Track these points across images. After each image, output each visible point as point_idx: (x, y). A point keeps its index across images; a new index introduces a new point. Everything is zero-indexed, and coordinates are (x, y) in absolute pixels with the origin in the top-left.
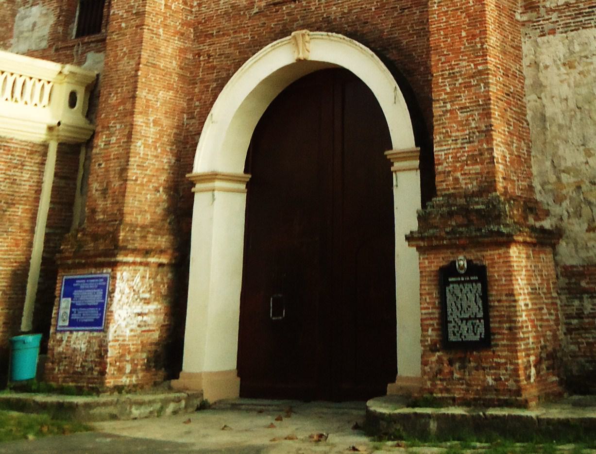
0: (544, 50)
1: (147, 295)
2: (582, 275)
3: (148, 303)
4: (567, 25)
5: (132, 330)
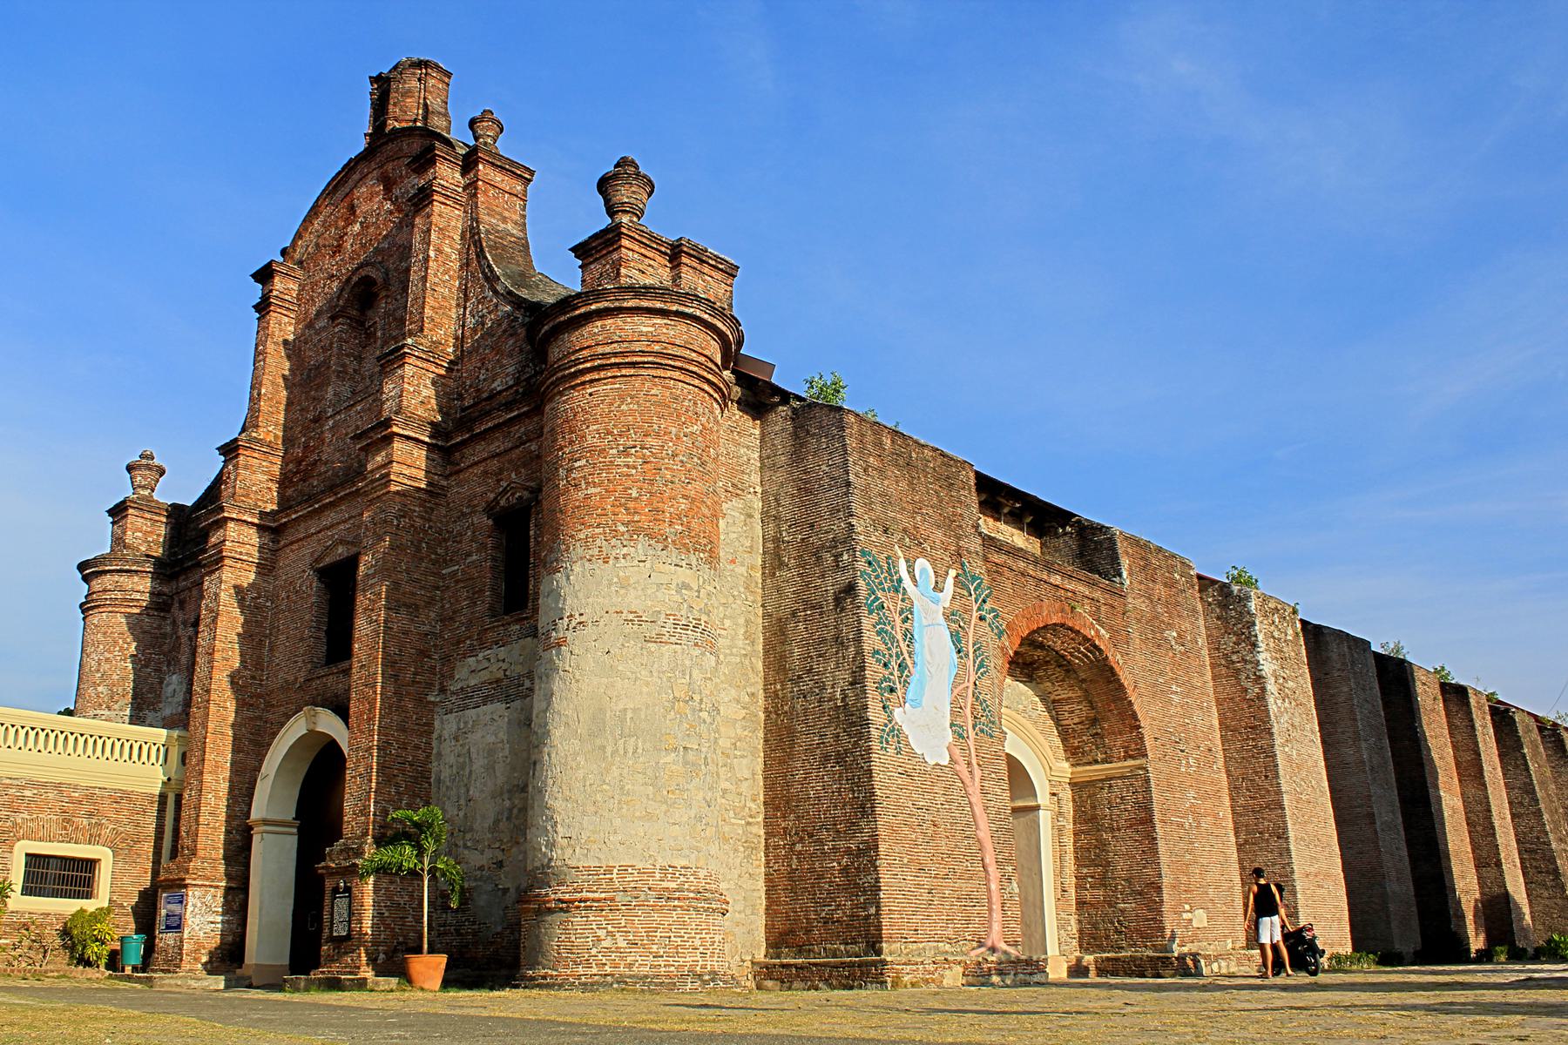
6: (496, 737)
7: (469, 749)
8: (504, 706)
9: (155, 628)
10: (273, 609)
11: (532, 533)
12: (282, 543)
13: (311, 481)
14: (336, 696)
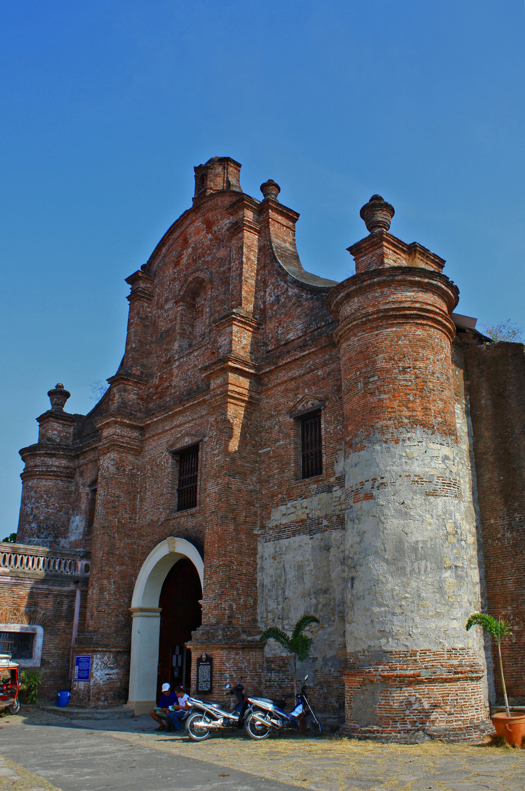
0: (266, 550)
1: (112, 666)
2: (272, 661)
3: (113, 669)
4: (275, 537)
5: (103, 681)
6: (304, 557)
7: (284, 565)
8: (308, 536)
9: (65, 488)
10: (141, 476)
11: (322, 426)
12: (147, 436)
13: (165, 398)
14: (187, 530)
